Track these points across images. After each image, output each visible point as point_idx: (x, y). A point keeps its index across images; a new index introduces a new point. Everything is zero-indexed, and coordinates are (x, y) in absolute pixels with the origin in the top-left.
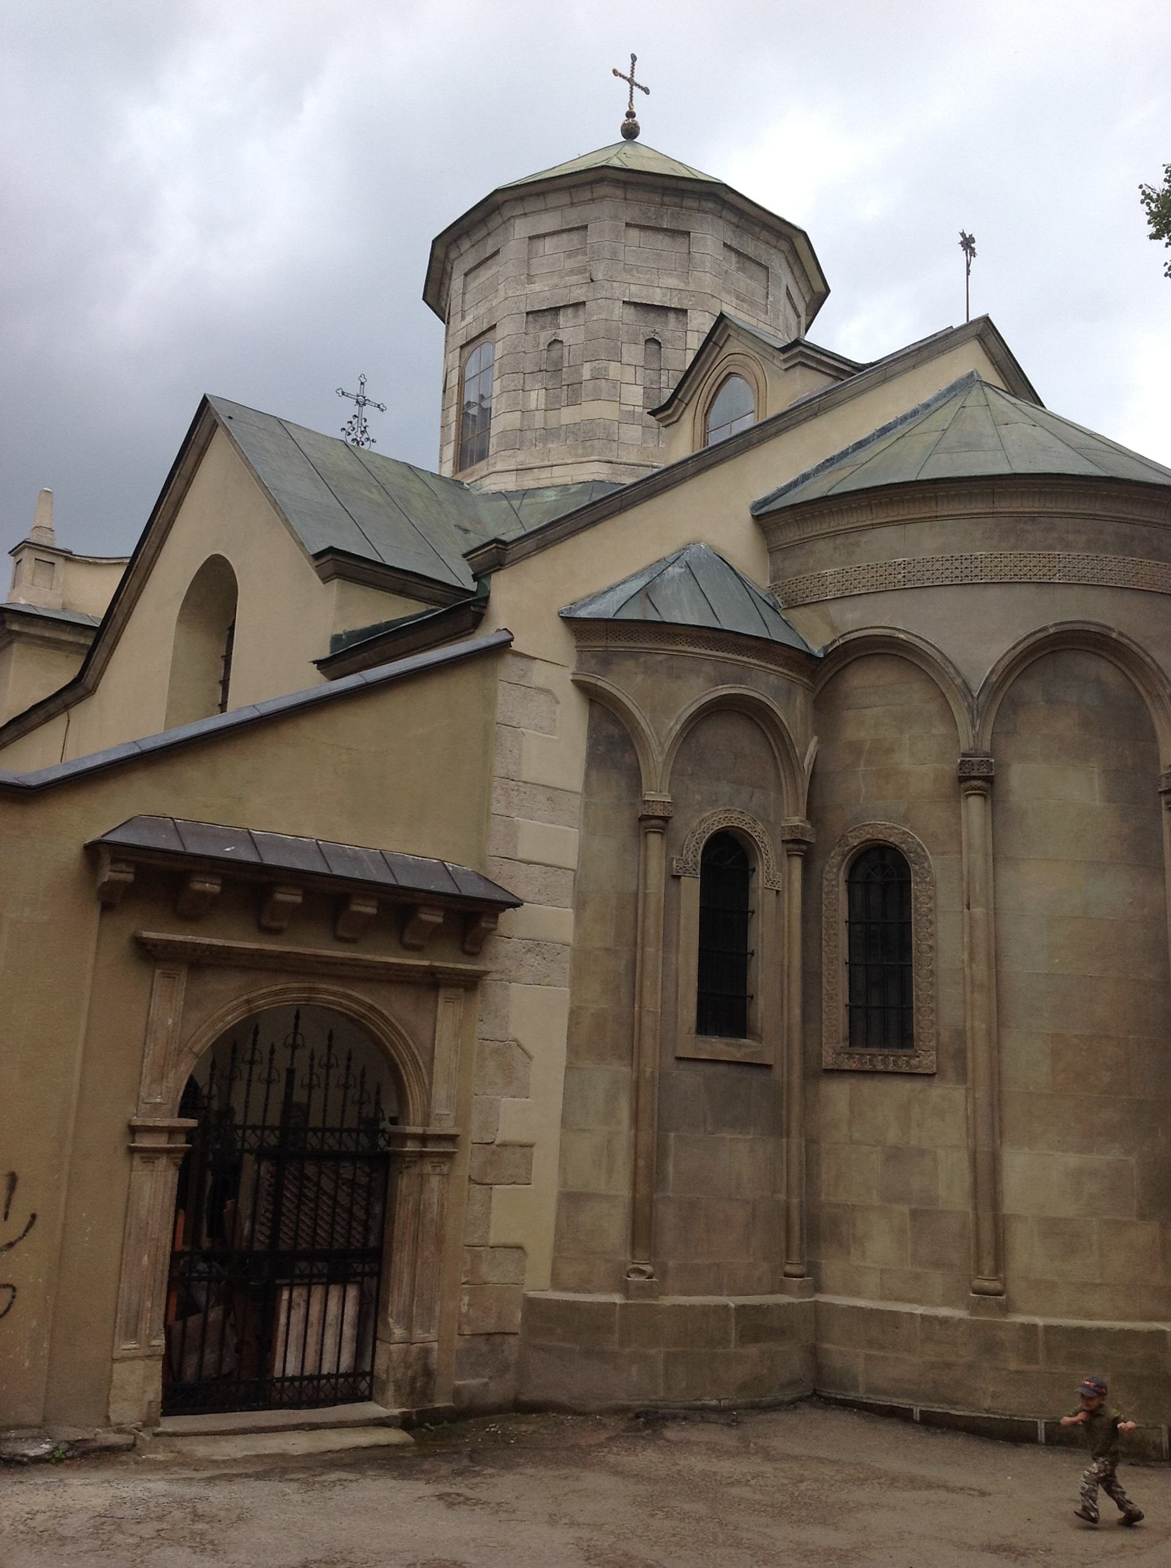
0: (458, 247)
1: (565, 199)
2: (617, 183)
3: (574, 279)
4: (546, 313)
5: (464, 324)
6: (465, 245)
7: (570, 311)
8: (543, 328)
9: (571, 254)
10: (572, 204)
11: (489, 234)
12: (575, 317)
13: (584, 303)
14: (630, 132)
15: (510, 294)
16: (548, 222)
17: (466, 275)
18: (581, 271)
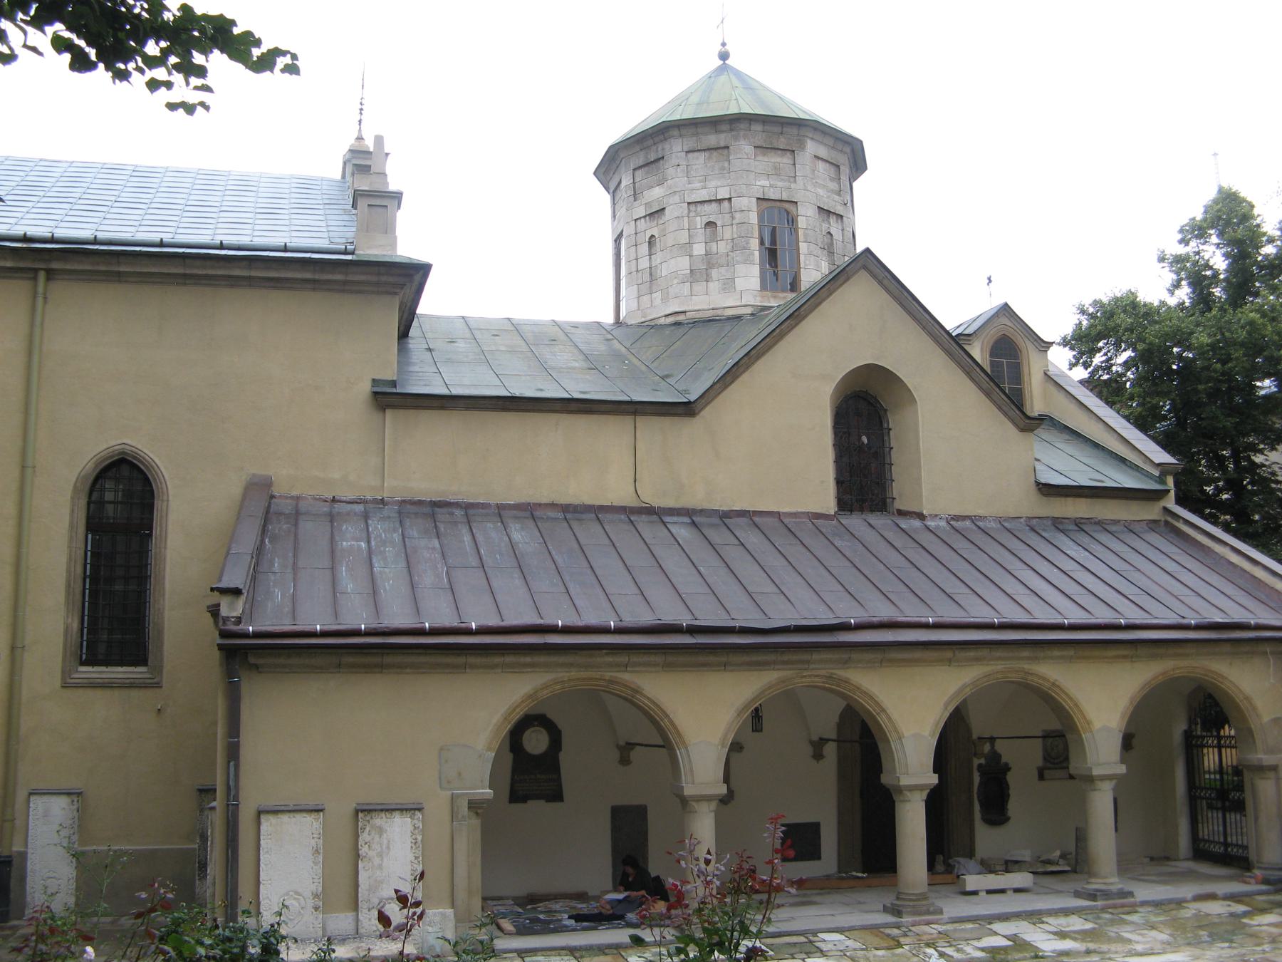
0: (750, 124)
1: (831, 142)
2: (853, 151)
3: (837, 198)
4: (825, 212)
5: (758, 183)
6: (757, 127)
7: (834, 217)
8: (823, 220)
9: (832, 179)
10: (833, 148)
11: (782, 133)
12: (837, 222)
13: (842, 217)
14: (724, 56)
15: (809, 188)
16: (823, 152)
17: (755, 147)
18: (839, 193)
